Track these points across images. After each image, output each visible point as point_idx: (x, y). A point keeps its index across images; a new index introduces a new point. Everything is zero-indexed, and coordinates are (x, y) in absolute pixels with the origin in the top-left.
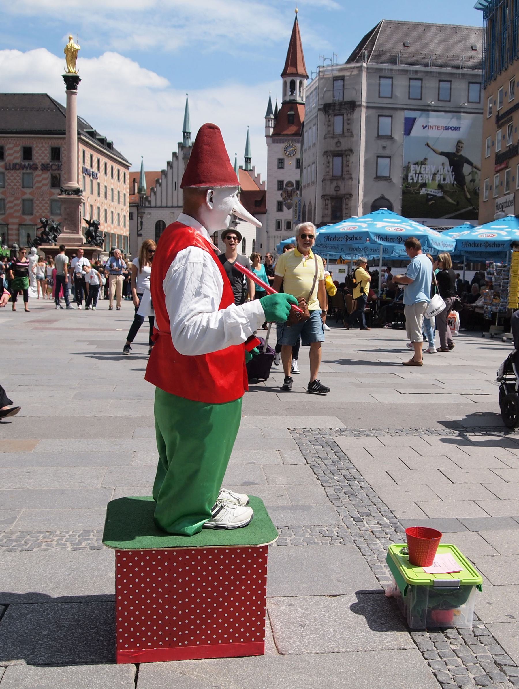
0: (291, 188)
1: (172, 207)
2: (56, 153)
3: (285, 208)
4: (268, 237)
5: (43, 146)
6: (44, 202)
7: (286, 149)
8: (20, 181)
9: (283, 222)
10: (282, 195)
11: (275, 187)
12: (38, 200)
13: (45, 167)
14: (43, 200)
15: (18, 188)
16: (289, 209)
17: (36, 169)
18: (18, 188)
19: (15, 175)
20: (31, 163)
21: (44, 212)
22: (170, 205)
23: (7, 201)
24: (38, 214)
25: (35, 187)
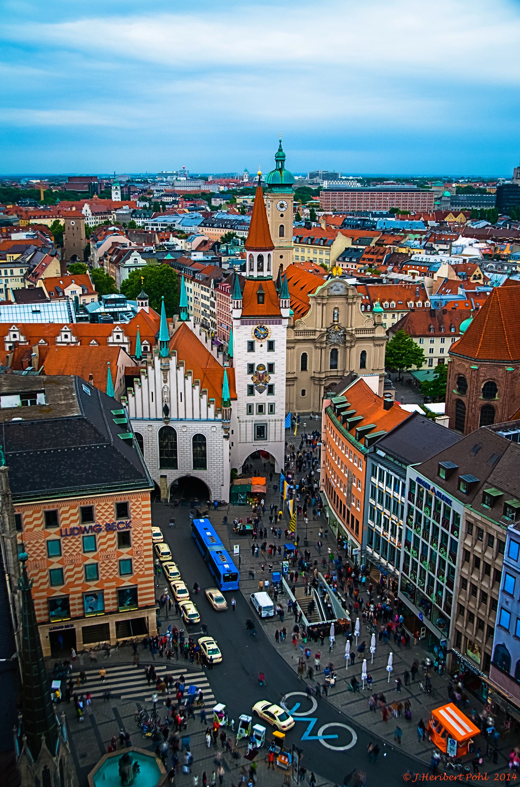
0: (263, 371)
1: (150, 419)
2: (122, 510)
3: (256, 392)
4: (240, 422)
5: (106, 504)
6: (110, 564)
7: (256, 331)
8: (80, 546)
9: (255, 406)
10: (252, 378)
11: (246, 370)
12: (103, 563)
13: (110, 528)
14: (110, 562)
15: (78, 554)
16: (261, 393)
17: (100, 530)
18: (78, 554)
19: (73, 540)
20: (93, 525)
21: (111, 575)
22: (146, 416)
23: (64, 571)
24: (104, 578)
25: (99, 550)
